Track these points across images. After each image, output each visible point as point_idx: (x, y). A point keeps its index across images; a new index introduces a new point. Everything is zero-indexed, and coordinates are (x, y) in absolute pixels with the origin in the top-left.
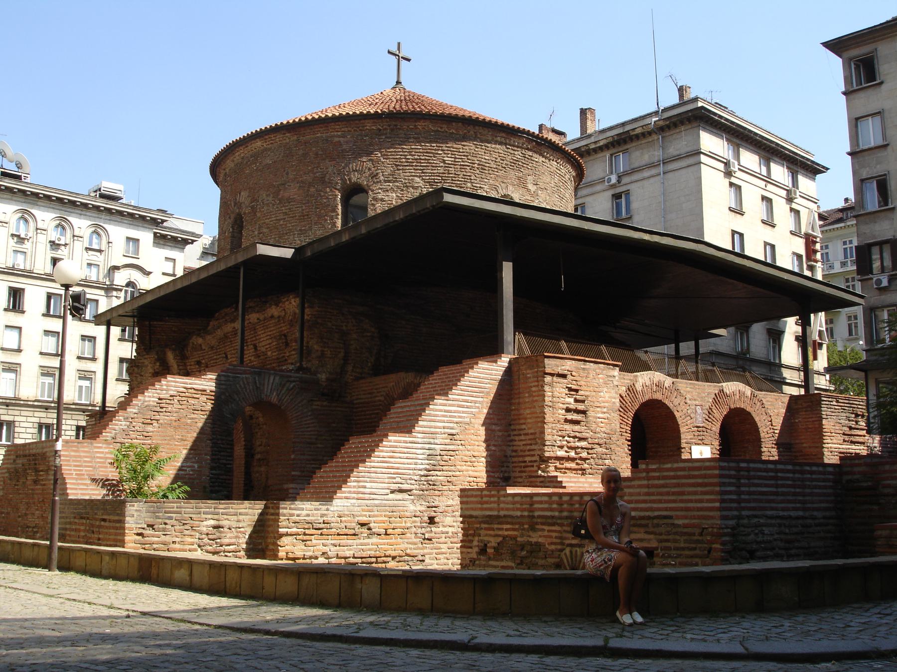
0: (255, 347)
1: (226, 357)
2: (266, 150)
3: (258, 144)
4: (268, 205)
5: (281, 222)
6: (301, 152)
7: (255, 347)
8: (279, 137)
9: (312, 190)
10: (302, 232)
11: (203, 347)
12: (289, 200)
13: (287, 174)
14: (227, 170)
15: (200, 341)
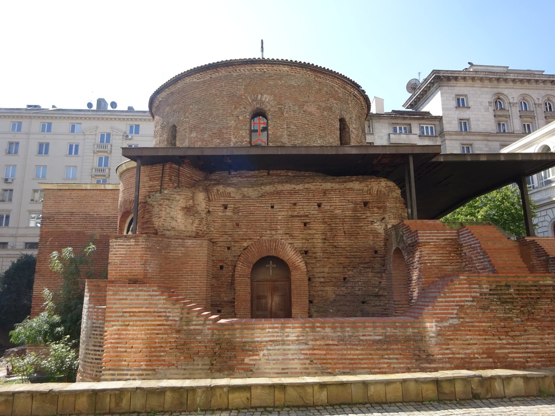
0: (319, 205)
1: (272, 207)
2: (290, 75)
3: (286, 69)
4: (294, 111)
5: (307, 126)
6: (317, 87)
7: (319, 205)
8: (303, 71)
9: (325, 113)
10: (321, 137)
11: (232, 195)
12: (311, 114)
13: (309, 97)
14: (235, 74)
15: (230, 190)
